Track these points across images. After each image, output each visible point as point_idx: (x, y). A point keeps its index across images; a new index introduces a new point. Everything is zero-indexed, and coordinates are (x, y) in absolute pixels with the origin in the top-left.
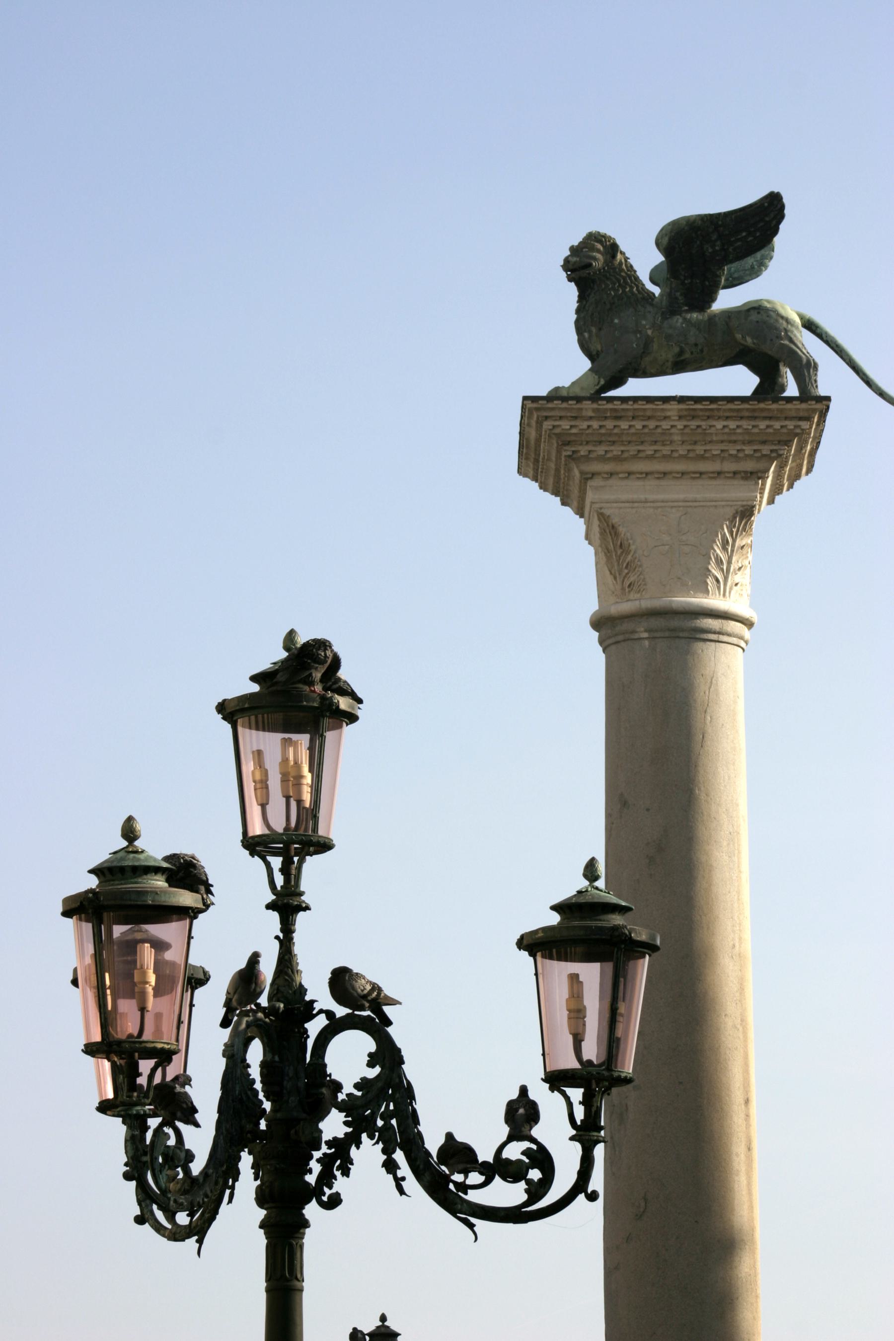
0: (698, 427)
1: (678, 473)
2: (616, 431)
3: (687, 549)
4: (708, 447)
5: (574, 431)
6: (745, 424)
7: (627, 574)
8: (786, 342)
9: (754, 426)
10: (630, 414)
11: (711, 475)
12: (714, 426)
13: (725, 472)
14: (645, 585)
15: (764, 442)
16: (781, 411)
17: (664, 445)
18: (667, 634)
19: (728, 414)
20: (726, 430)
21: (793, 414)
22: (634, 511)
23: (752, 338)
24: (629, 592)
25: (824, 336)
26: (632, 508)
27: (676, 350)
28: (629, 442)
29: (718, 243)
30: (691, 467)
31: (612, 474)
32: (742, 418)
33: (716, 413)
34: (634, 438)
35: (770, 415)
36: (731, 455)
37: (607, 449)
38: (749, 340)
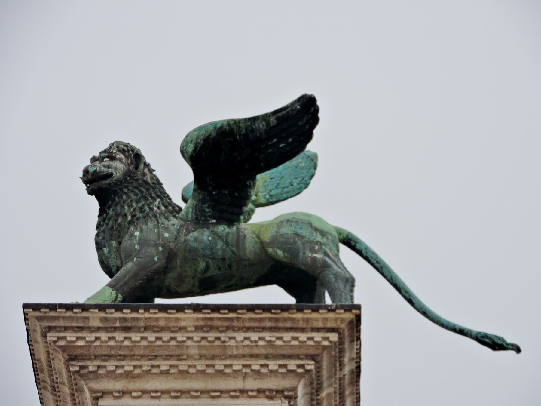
0: (218, 338)
1: (196, 391)
4: (228, 362)
5: (80, 343)
6: (267, 336)
10: (142, 324)
11: (233, 394)
12: (234, 338)
13: (247, 391)
15: (290, 357)
16: (307, 320)
19: (248, 324)
21: (320, 325)
23: (284, 251)
25: (364, 252)
27: (202, 265)
28: (142, 356)
30: (211, 385)
31: (124, 393)
32: (264, 329)
34: (147, 352)
35: (295, 325)
36: (253, 371)
37: (117, 363)
38: (280, 252)
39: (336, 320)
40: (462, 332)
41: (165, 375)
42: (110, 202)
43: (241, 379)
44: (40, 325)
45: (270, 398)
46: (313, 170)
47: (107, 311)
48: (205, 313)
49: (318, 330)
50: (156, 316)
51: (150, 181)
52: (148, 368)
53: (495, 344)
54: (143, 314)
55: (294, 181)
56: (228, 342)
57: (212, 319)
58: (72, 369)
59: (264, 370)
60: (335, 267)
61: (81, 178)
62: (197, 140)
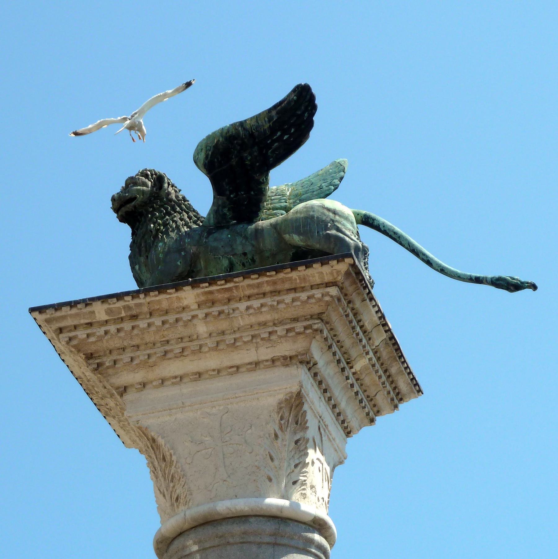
1: (214, 370)
2: (135, 332)
4: (237, 335)
7: (174, 487)
8: (334, 232)
9: (279, 302)
10: (145, 309)
12: (238, 308)
14: (191, 494)
15: (296, 320)
16: (304, 279)
18: (217, 542)
19: (248, 292)
21: (318, 281)
23: (299, 234)
24: (178, 507)
29: (256, 148)
31: (144, 385)
32: (264, 294)
34: (158, 338)
36: (263, 339)
37: (132, 355)
39: (332, 273)
40: (478, 280)
41: (179, 359)
42: (138, 224)
43: (253, 350)
47: (109, 300)
48: (203, 288)
49: (318, 286)
50: (157, 298)
51: (174, 198)
53: (512, 286)
54: (144, 298)
55: (323, 184)
57: (211, 293)
60: (347, 239)
62: (206, 148)
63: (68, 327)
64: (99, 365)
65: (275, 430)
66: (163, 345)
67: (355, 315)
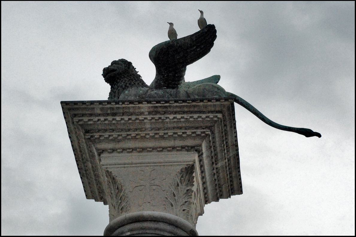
0: (160, 118)
1: (150, 148)
3: (154, 187)
4: (166, 132)
6: (185, 116)
7: (121, 203)
9: (191, 117)
10: (121, 111)
12: (168, 118)
15: (197, 128)
16: (206, 107)
17: (141, 131)
20: (175, 120)
21: (213, 109)
22: (126, 169)
24: (121, 213)
26: (125, 167)
31: (113, 150)
32: (184, 112)
33: (169, 109)
37: (110, 134)
44: (70, 113)
45: (188, 151)
46: (217, 80)
48: (152, 104)
49: (212, 112)
50: (128, 106)
52: (125, 136)
54: (121, 105)
56: (165, 120)
57: (156, 107)
58: (87, 137)
59: (184, 135)
61: (102, 75)
63: (78, 114)
64: (92, 136)
65: (178, 182)
66: (126, 131)
67: (225, 134)
